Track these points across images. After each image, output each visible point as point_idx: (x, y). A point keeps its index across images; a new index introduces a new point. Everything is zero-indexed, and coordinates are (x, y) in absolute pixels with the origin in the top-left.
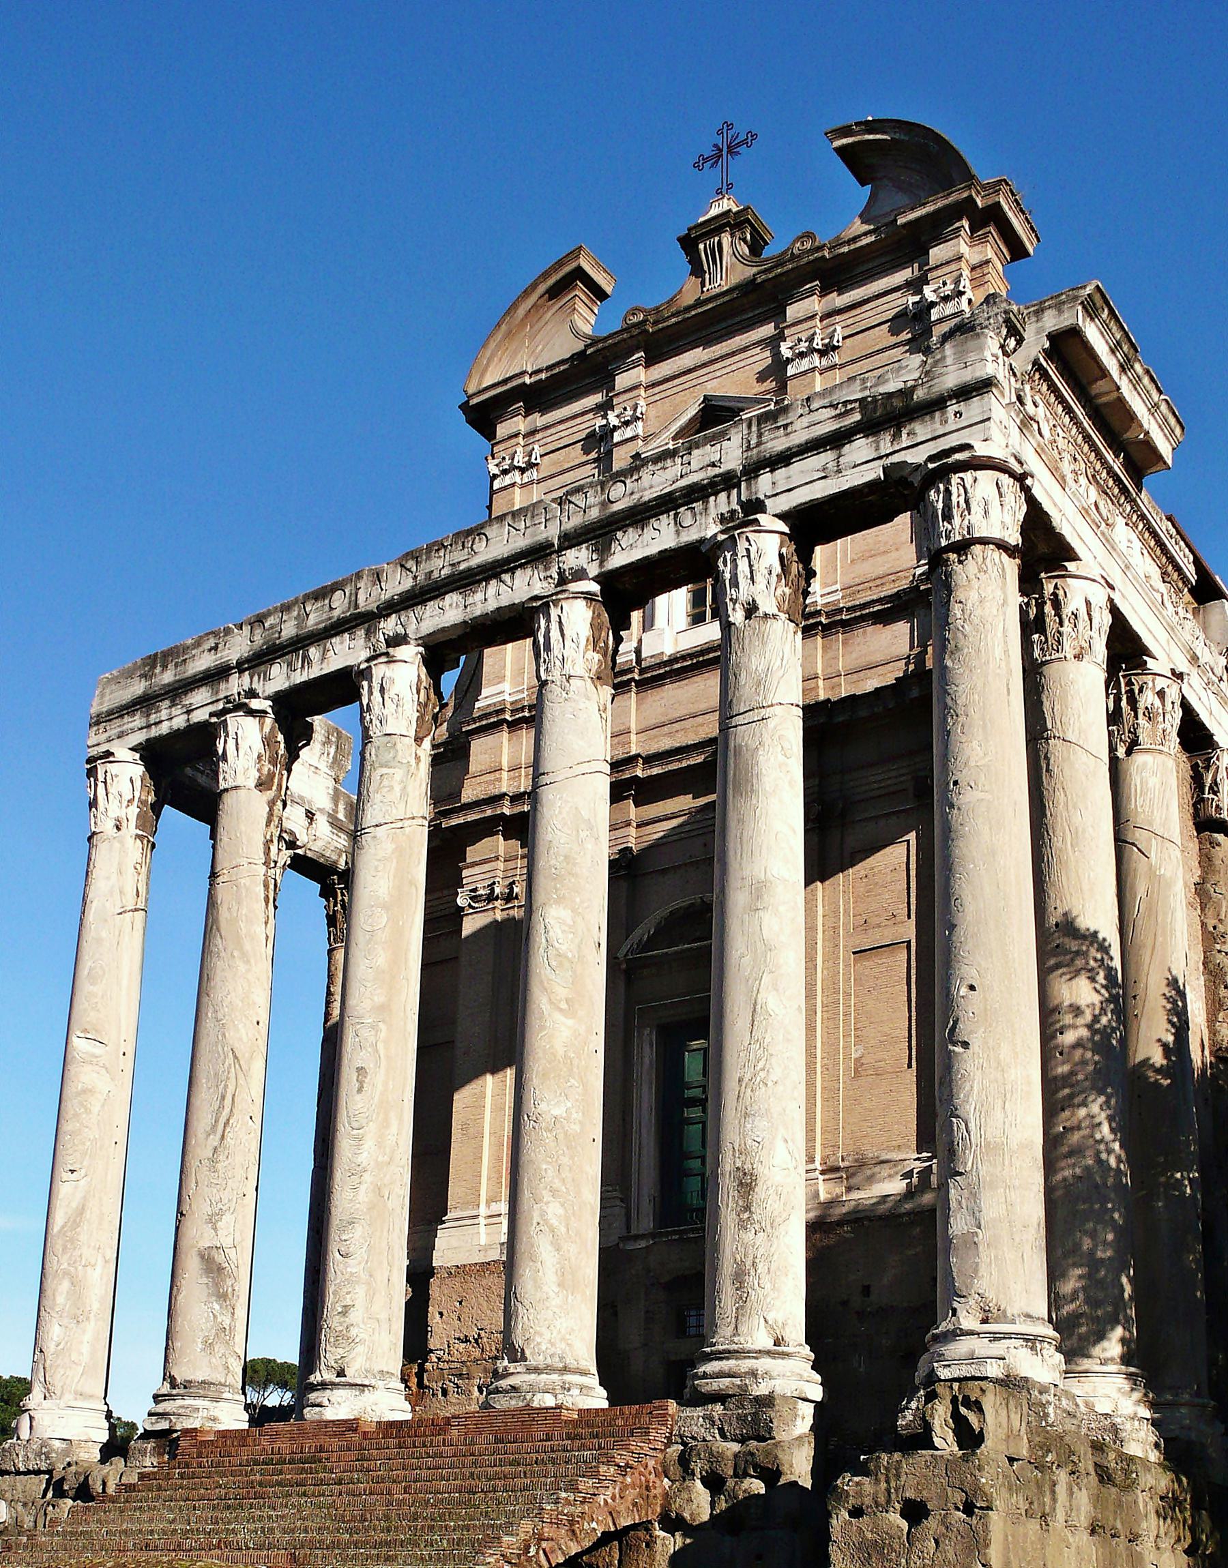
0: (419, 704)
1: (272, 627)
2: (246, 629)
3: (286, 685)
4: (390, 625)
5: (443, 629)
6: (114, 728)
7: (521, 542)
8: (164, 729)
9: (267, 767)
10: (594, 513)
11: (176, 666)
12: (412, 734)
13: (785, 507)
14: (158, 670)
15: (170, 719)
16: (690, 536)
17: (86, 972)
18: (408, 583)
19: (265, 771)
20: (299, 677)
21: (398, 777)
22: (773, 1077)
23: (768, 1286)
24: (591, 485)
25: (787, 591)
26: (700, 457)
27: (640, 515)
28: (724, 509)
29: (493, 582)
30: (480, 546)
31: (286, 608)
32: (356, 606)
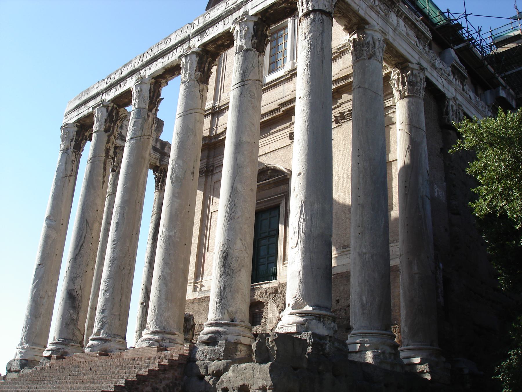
0: (150, 97)
4: (142, 73)
5: (156, 71)
6: (69, 117)
7: (179, 39)
8: (82, 115)
9: (108, 124)
12: (147, 107)
15: (84, 111)
19: (107, 125)
21: (140, 122)
22: (237, 215)
23: (230, 297)
25: (256, 41)
28: (237, 16)
31: (117, 71)
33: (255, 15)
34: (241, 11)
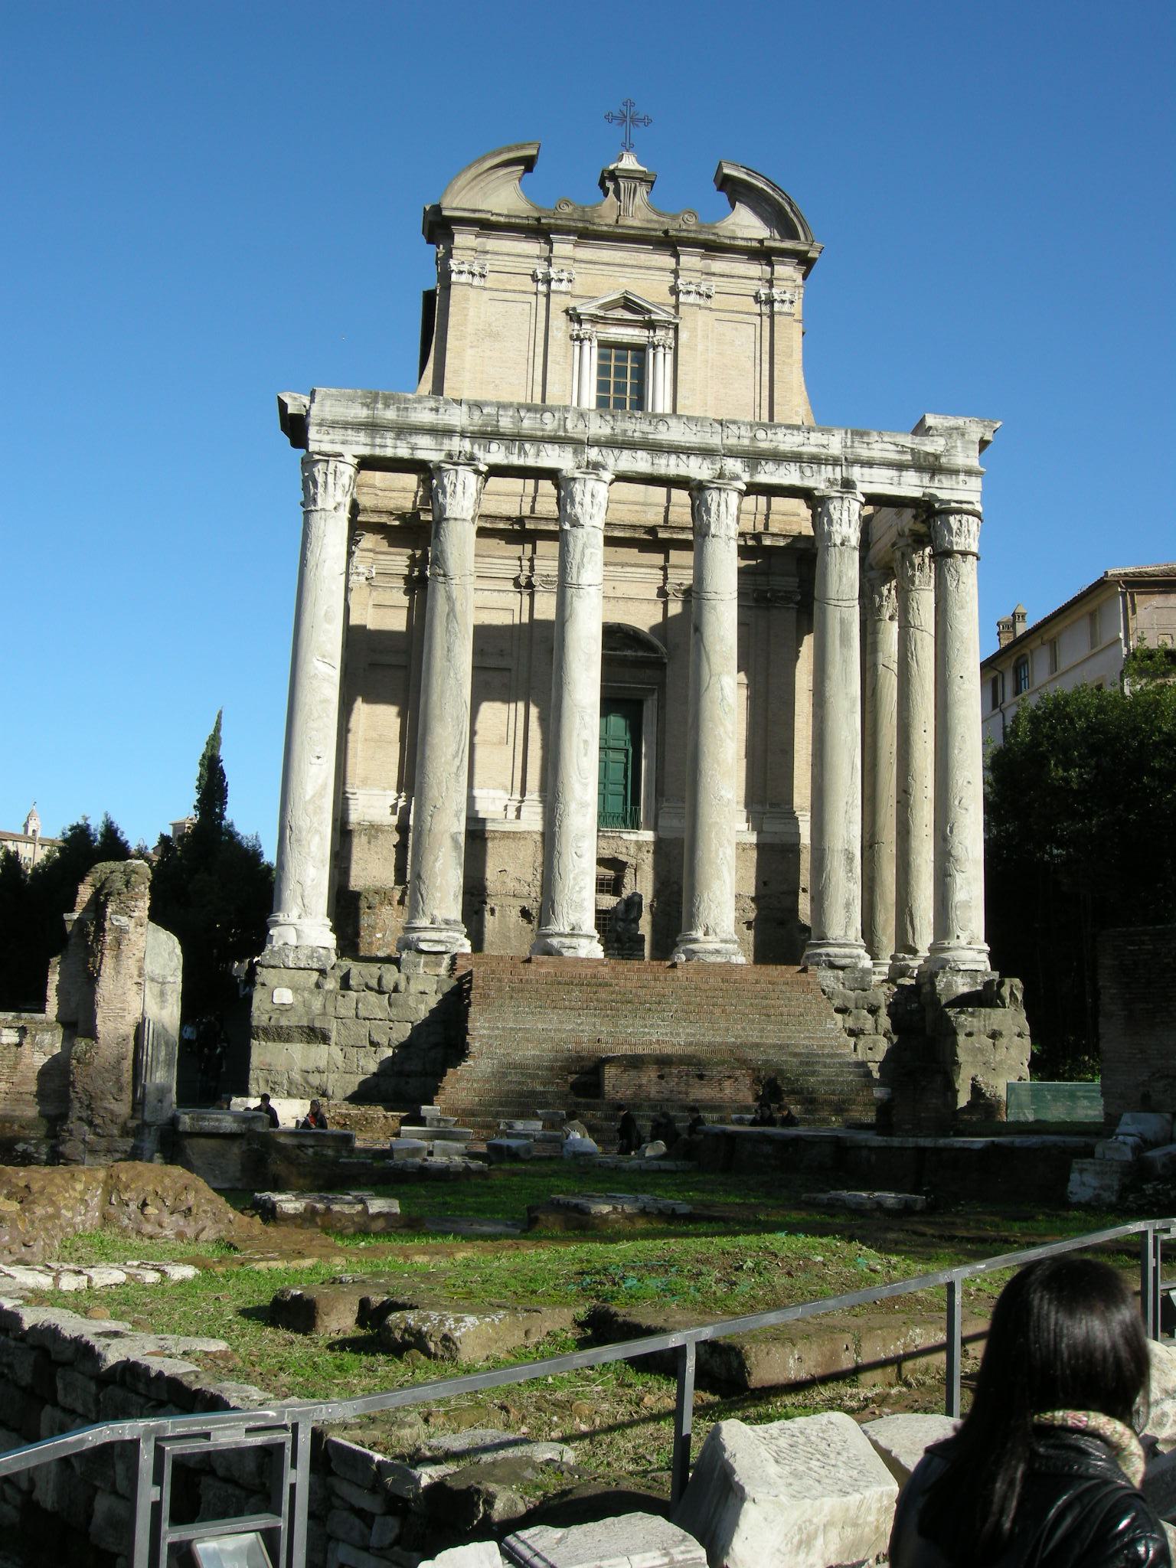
1: (489, 415)
2: (465, 408)
3: (505, 462)
4: (593, 454)
6: (338, 434)
8: (389, 452)
10: (746, 442)
11: (398, 409)
13: (868, 491)
14: (380, 406)
16: (809, 483)
17: (323, 613)
18: (606, 431)
20: (516, 460)
24: (744, 423)
26: (816, 437)
27: (778, 457)
28: (832, 477)
29: (674, 457)
30: (662, 427)
32: (566, 430)
33: (864, 494)
34: (838, 473)
